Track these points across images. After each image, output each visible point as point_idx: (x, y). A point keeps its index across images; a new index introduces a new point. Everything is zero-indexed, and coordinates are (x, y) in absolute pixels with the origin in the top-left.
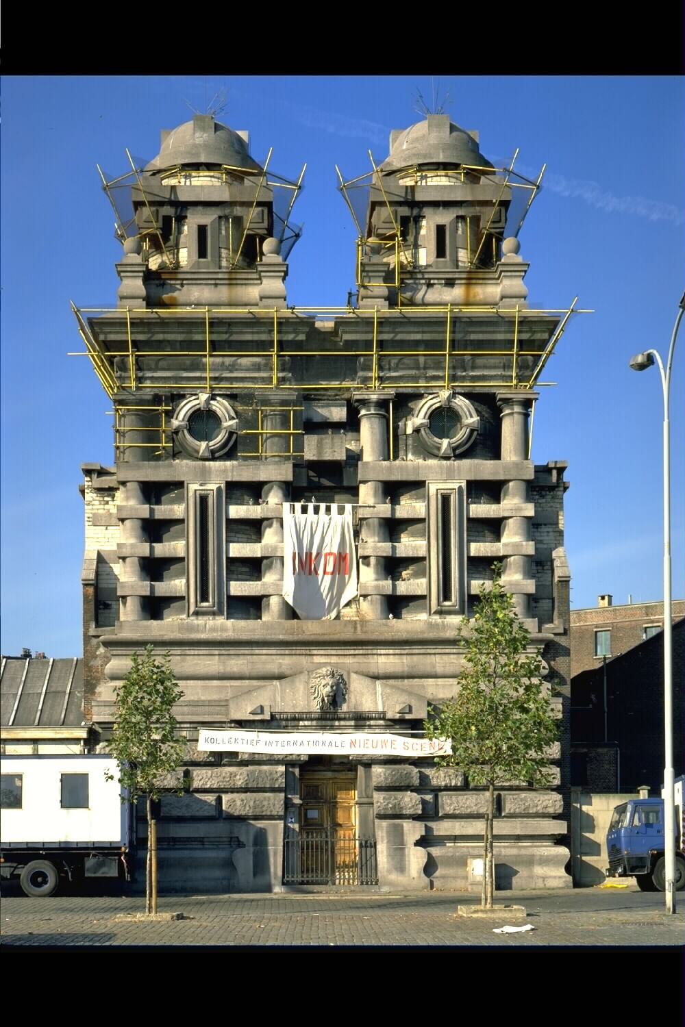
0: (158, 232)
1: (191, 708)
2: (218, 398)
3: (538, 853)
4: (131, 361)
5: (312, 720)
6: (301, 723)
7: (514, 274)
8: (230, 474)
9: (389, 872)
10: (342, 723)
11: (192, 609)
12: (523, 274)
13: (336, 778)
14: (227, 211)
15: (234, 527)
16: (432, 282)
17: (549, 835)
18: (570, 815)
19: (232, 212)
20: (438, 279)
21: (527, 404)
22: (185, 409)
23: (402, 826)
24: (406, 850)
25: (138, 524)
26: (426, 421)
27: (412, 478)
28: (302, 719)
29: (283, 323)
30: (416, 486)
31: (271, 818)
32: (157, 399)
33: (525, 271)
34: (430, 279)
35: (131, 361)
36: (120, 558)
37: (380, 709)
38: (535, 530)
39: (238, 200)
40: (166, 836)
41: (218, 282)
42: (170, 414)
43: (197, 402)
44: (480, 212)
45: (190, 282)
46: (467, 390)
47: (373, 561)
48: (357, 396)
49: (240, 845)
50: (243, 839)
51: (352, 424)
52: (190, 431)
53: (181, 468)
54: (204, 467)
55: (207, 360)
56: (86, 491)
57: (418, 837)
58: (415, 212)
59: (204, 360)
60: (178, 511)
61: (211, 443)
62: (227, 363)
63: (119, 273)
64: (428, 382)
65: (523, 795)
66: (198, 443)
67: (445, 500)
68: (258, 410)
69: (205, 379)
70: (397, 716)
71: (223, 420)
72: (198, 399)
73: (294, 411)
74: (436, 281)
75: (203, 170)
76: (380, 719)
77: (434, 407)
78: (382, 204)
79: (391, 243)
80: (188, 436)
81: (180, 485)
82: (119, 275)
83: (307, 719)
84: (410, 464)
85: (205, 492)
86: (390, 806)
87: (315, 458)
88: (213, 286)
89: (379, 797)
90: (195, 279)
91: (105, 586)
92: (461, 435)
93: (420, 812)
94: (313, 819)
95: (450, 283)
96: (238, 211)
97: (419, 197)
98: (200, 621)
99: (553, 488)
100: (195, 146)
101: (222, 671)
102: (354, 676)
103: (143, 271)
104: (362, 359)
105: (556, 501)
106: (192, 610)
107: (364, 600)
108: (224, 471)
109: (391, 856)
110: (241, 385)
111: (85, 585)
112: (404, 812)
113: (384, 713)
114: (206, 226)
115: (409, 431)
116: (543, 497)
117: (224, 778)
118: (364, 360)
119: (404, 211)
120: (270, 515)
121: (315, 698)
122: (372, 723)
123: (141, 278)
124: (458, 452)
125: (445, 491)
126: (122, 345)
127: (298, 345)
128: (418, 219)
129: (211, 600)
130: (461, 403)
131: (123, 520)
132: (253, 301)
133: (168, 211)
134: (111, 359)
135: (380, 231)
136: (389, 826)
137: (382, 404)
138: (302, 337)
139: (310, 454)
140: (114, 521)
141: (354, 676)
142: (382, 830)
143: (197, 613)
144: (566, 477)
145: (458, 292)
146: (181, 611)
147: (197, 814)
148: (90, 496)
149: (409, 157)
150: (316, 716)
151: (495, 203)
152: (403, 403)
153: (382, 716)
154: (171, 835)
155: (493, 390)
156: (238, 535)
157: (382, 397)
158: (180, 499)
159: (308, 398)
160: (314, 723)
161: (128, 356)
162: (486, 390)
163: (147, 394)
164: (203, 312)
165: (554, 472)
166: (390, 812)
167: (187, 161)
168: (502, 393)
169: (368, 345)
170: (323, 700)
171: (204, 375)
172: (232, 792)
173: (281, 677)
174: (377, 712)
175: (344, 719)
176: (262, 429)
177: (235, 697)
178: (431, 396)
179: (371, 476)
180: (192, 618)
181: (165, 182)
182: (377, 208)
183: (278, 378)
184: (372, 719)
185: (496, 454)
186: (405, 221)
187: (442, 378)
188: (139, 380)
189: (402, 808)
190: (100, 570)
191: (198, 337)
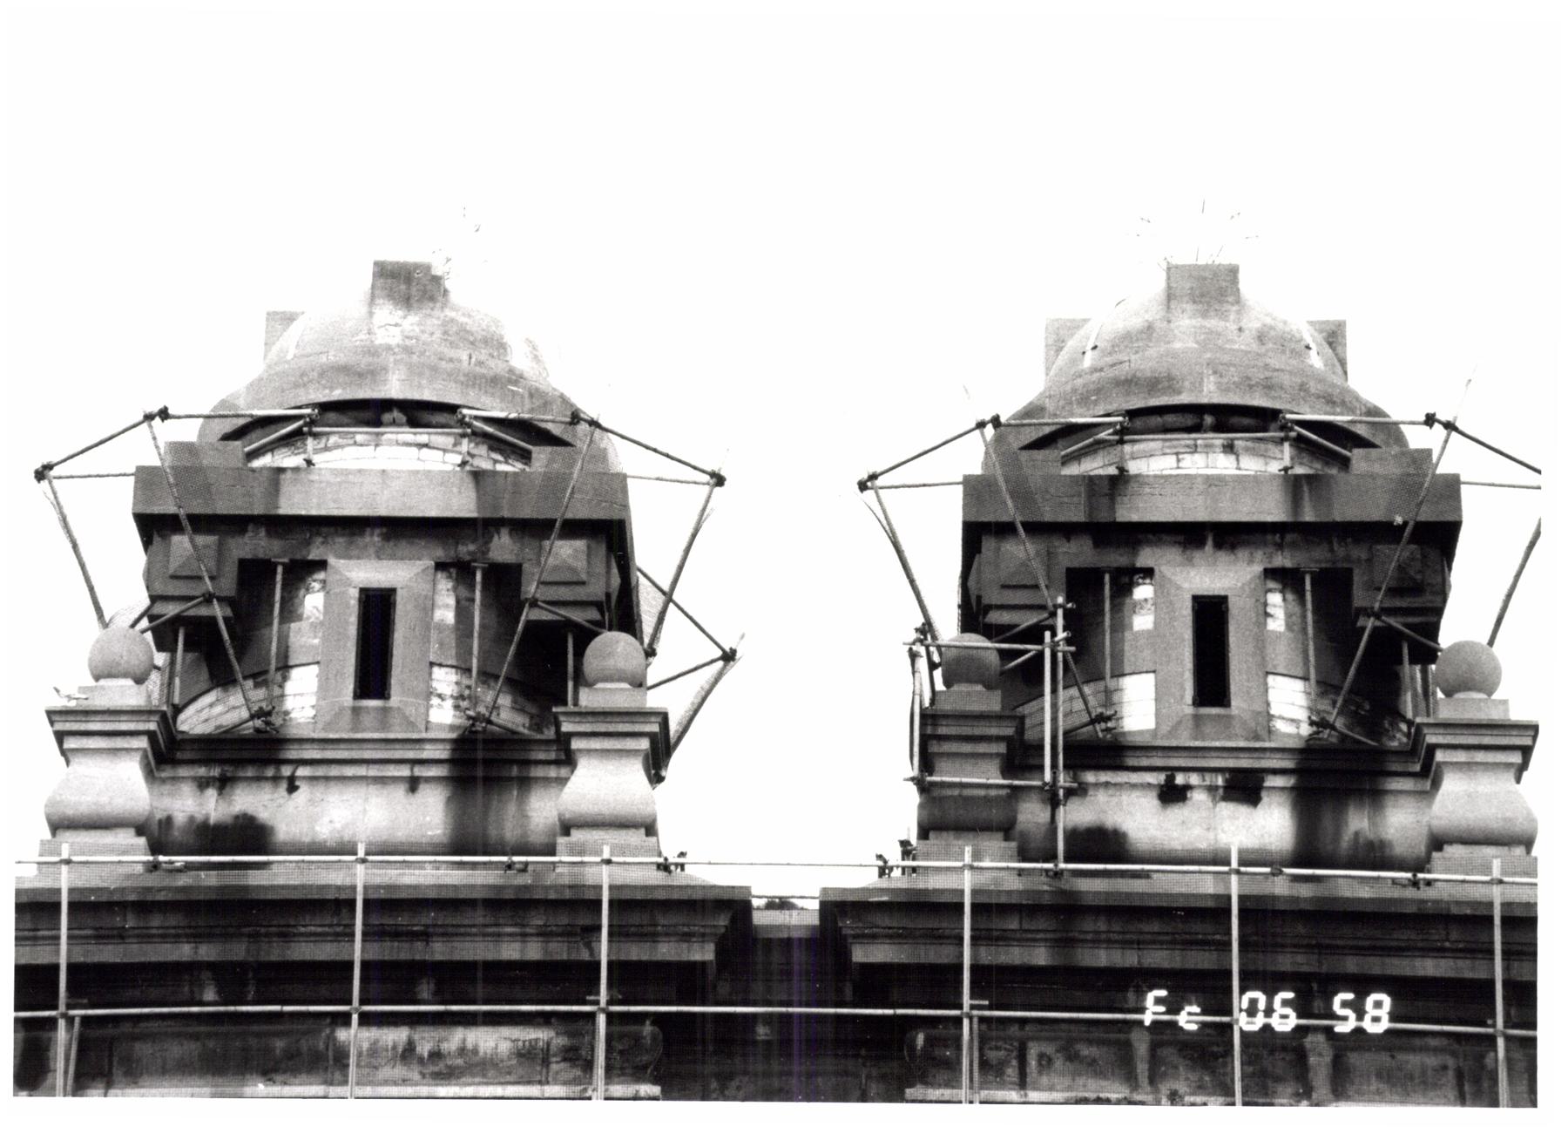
7: (1480, 756)
12: (1516, 758)
14: (466, 549)
16: (1180, 779)
20: (1201, 770)
29: (639, 910)
34: (1172, 771)
39: (506, 513)
41: (419, 771)
44: (1347, 558)
45: (320, 771)
55: (354, 1036)
58: (1116, 558)
59: (342, 1035)
62: (424, 1048)
63: (60, 736)
74: (1194, 779)
75: (394, 423)
78: (1004, 530)
82: (60, 742)
88: (399, 791)
90: (337, 760)
95: (1244, 788)
96: (503, 548)
97: (1133, 511)
100: (372, 351)
103: (151, 735)
104: (920, 1039)
114: (393, 591)
119: (1079, 553)
123: (137, 757)
128: (1126, 579)
132: (536, 838)
135: (995, 617)
138: (704, 953)
145: (1270, 824)
149: (1098, 391)
161: (52, 1023)
164: (360, 877)
167: (338, 394)
181: (265, 461)
182: (988, 544)
186: (1082, 584)
191: (324, 952)
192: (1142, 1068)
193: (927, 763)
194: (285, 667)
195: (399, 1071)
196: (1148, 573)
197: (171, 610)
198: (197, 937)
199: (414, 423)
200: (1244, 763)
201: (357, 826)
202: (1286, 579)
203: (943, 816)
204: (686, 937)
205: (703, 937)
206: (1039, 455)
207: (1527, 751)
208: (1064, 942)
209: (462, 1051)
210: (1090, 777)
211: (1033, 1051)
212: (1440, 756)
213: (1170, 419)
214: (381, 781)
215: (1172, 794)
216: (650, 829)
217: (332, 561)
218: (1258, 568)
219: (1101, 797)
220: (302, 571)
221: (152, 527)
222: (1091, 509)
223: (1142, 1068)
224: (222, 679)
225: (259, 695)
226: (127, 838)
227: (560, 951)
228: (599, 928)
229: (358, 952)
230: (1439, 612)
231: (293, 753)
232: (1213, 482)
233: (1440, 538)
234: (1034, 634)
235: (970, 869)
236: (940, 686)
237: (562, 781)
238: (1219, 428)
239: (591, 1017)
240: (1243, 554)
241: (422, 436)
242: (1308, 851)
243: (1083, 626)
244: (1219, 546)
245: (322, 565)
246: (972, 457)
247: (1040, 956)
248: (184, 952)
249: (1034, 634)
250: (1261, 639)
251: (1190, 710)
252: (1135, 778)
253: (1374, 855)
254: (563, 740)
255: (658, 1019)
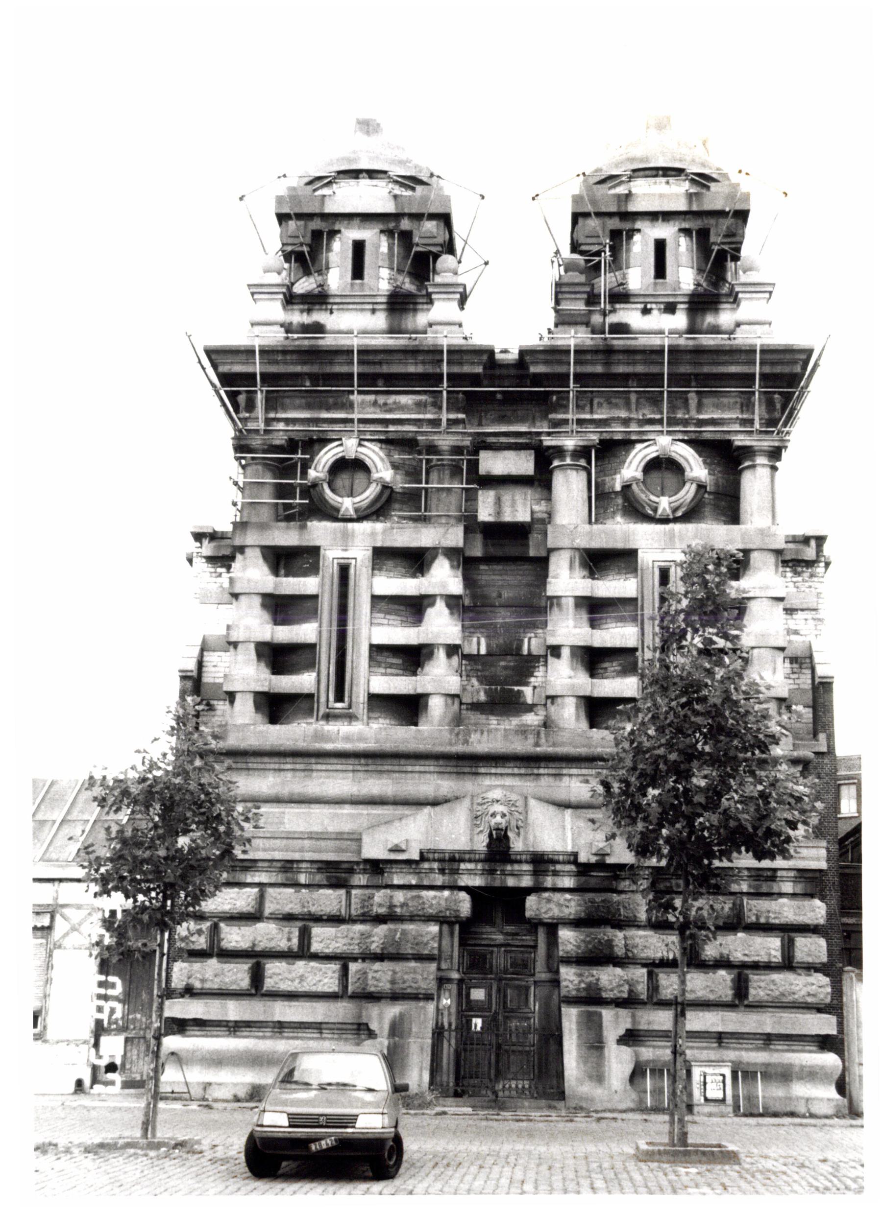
0: (305, 249)
1: (313, 842)
2: (366, 443)
3: (797, 1062)
4: (260, 398)
5: (476, 861)
6: (463, 866)
8: (379, 537)
9: (580, 1081)
10: (516, 867)
11: (323, 710)
12: (767, 295)
13: (508, 945)
14: (392, 225)
15: (383, 605)
16: (649, 306)
17: (812, 1036)
18: (842, 1009)
19: (397, 226)
20: (656, 303)
21: (775, 454)
22: (326, 457)
23: (600, 1015)
24: (606, 1051)
25: (257, 601)
26: (639, 475)
27: (620, 545)
28: (462, 860)
29: (457, 354)
30: (621, 559)
31: (415, 997)
32: (292, 445)
33: (771, 293)
34: (646, 303)
35: (260, 398)
36: (230, 643)
37: (569, 849)
38: (789, 617)
39: (406, 211)
40: (269, 1019)
41: (376, 307)
42: (306, 465)
43: (340, 449)
45: (341, 306)
46: (693, 436)
47: (566, 652)
48: (548, 441)
49: (371, 1034)
50: (374, 1026)
51: (541, 480)
52: (330, 485)
53: (319, 532)
54: (346, 529)
55: (356, 398)
56: (194, 560)
57: (622, 1032)
58: (627, 226)
59: (351, 397)
60: (307, 585)
61: (357, 499)
63: (253, 294)
64: (641, 426)
65: (776, 976)
66: (339, 499)
67: (664, 575)
68: (421, 460)
69: (351, 421)
70: (593, 859)
71: (373, 470)
72: (341, 445)
73: (469, 461)
74: (654, 306)
76: (569, 862)
77: (648, 458)
78: (586, 215)
79: (597, 259)
80: (327, 491)
81: (315, 551)
83: (470, 861)
84: (619, 531)
85: (346, 561)
86: (583, 985)
87: (491, 519)
88: (369, 314)
89: (569, 975)
90: (347, 303)
91: (211, 680)
92: (688, 493)
93: (625, 995)
94: (477, 1001)
95: (670, 308)
96: (405, 224)
97: (632, 207)
98: (332, 727)
99: (810, 564)
101: (356, 793)
102: (532, 802)
103: (284, 294)
104: (554, 398)
105: (815, 579)
106: (321, 714)
107: (553, 703)
108: (369, 534)
109: (583, 1059)
110: (399, 428)
111: (184, 678)
112: (604, 995)
113: (575, 855)
115: (618, 488)
116: (798, 574)
117: (352, 939)
118: (558, 399)
119: (614, 223)
120: (431, 591)
121: (481, 832)
122: (559, 867)
124: (679, 513)
125: (663, 564)
126: (249, 379)
127: (475, 379)
128: (631, 233)
129: (346, 699)
130: (685, 453)
131: (236, 596)
133: (316, 224)
134: (232, 396)
135: (583, 248)
136: (580, 1015)
137: (583, 452)
138: (479, 370)
139: (485, 514)
140: (227, 597)
141: (532, 802)
142: (571, 1017)
143: (328, 717)
144: (827, 549)
146: (309, 712)
147: (314, 989)
148: (200, 564)
150: (482, 856)
151: (728, 213)
152: (610, 450)
153: (572, 858)
154: (276, 1019)
155: (728, 437)
156: (388, 617)
157: (581, 443)
158: (314, 569)
159: (482, 444)
160: (480, 866)
162: (718, 437)
163: (279, 440)
164: (355, 342)
165: (813, 543)
166: (584, 994)
168: (740, 440)
169: (562, 379)
170: (490, 835)
171: (350, 416)
172: (364, 960)
173: (435, 803)
174: (565, 853)
175: (520, 862)
176: (427, 483)
177: (372, 827)
178: (646, 444)
179: (565, 542)
180: (322, 723)
182: (581, 221)
183: (448, 420)
184: (558, 862)
185: (733, 516)
186: (615, 235)
187: (660, 422)
188: (268, 421)
189: (600, 989)
190: (205, 659)
191: (344, 369)
192: (633, 406)
193: (557, 302)
194: (328, 268)
195: (372, 409)
196: (639, 231)
197: (289, 248)
198: (304, 363)
199: (371, 178)
200: (671, 300)
201: (356, 326)
202: (686, 232)
203: (563, 320)
204: (473, 363)
205: (479, 364)
206: (598, 186)
207: (771, 293)
208: (607, 364)
209: (395, 403)
210: (618, 306)
211: (596, 401)
212: (740, 295)
213: (647, 173)
214: (362, 310)
215: (646, 311)
216: (460, 325)
217: (343, 230)
218: (676, 229)
219: (621, 312)
220: (333, 234)
221: (282, 218)
222: (619, 206)
223: (633, 406)
224: (307, 272)
225: (320, 278)
226: (277, 328)
227: (429, 369)
228: (442, 361)
229: (356, 369)
230: (741, 243)
231: (331, 300)
232: (661, 196)
233: (742, 215)
234: (598, 254)
235: (573, 338)
236: (562, 273)
237: (429, 310)
238: (664, 176)
239: (441, 392)
240: (672, 223)
241: (375, 182)
242: (692, 329)
243: (615, 250)
244: (663, 220)
245: (339, 232)
246: (576, 187)
247: (599, 369)
248: (298, 369)
249: (598, 254)
250: (677, 255)
251: (652, 280)
252: (634, 306)
253: (715, 330)
254: (429, 295)
255: (464, 392)
